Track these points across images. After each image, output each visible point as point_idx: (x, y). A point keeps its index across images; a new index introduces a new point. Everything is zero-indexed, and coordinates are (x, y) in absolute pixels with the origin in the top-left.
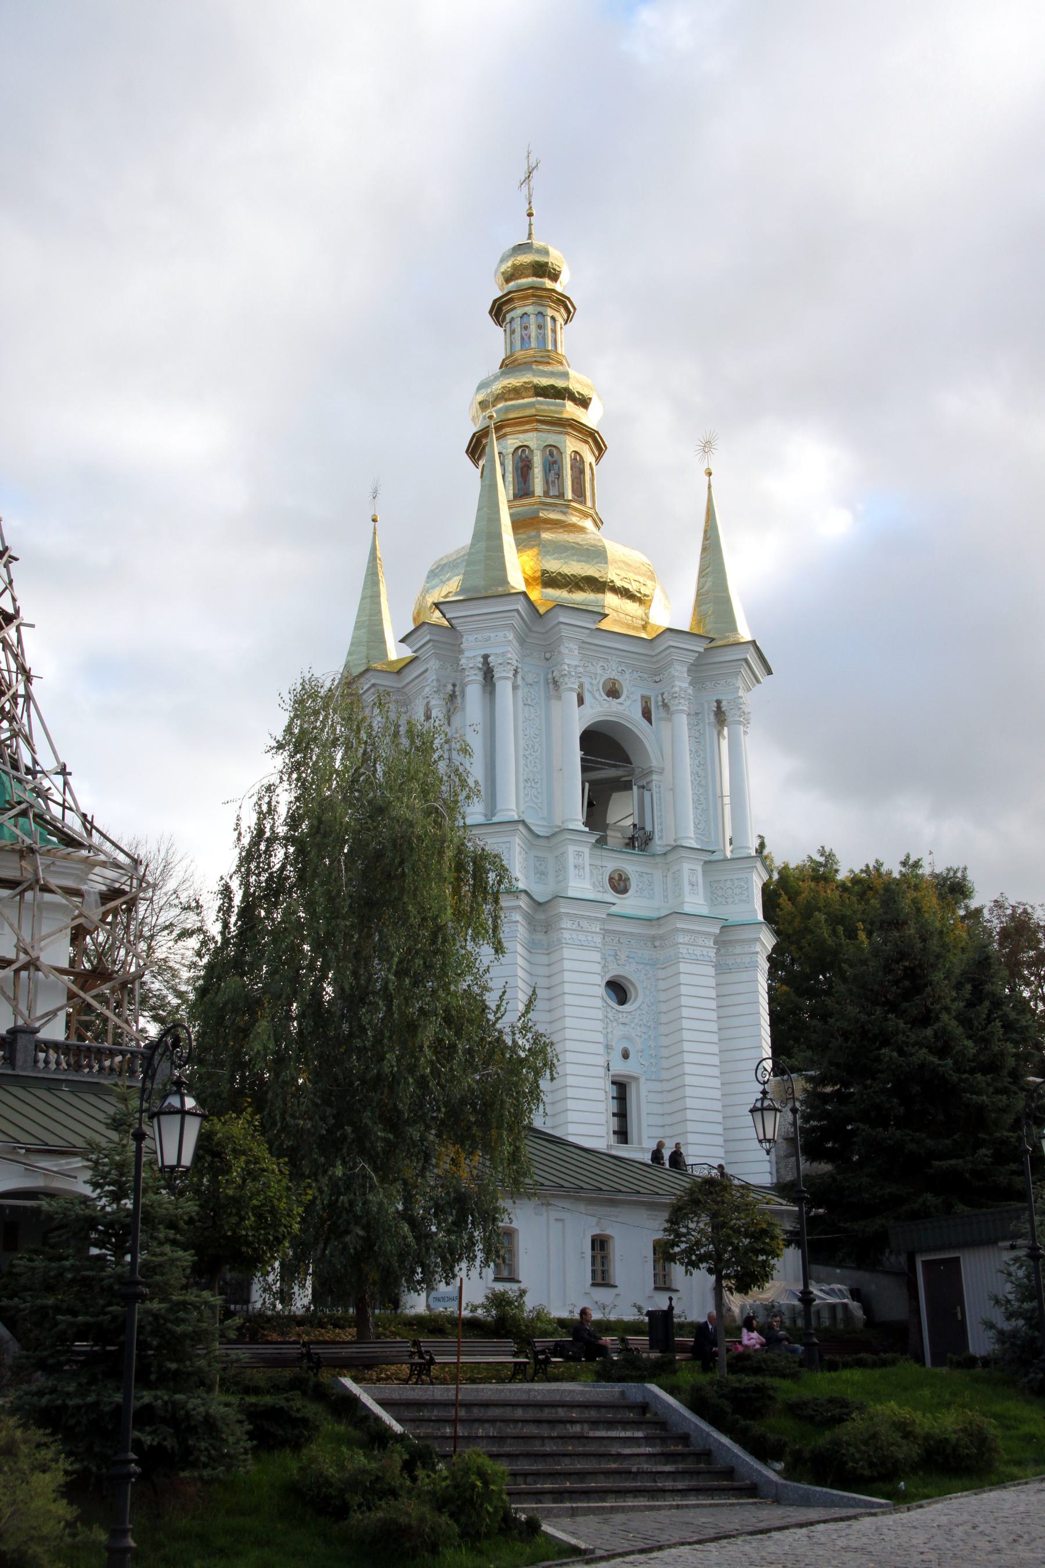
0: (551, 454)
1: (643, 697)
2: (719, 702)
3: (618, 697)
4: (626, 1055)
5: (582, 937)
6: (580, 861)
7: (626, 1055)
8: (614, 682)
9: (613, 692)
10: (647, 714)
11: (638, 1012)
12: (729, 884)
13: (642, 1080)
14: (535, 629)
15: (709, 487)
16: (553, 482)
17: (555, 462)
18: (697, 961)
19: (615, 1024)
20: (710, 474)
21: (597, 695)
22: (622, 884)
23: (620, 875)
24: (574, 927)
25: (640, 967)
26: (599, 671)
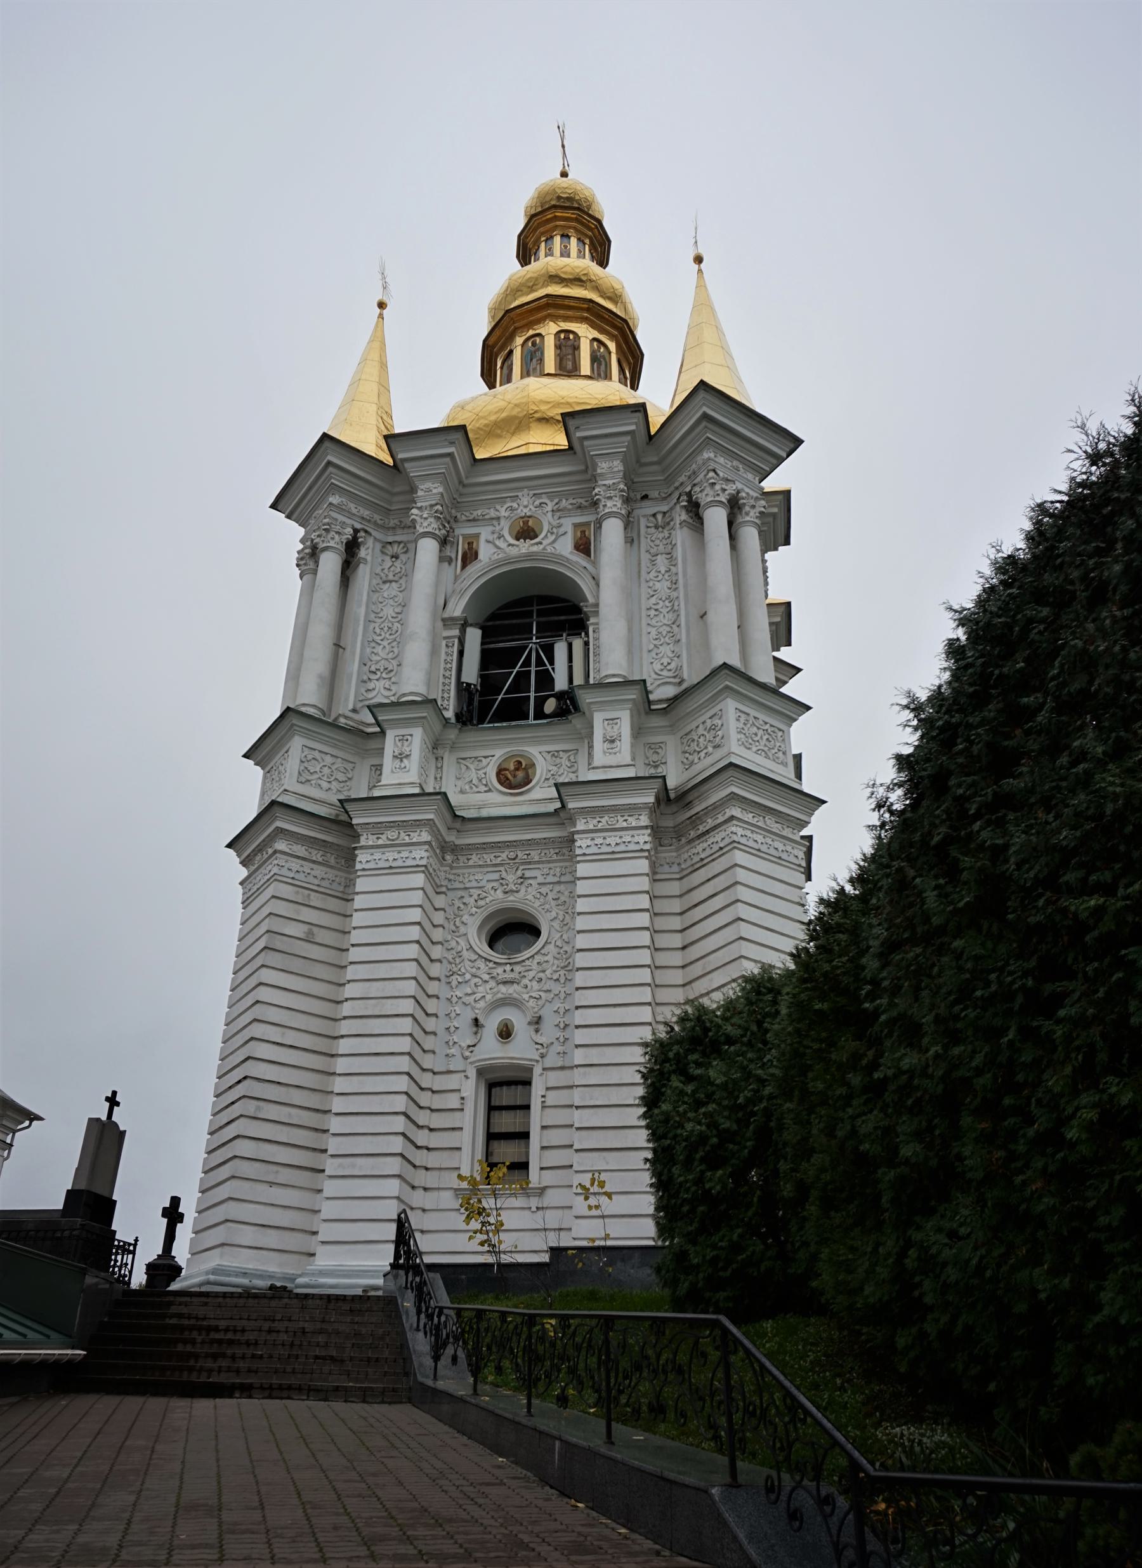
0: (534, 344)
1: (576, 526)
2: (689, 494)
3: (536, 536)
4: (505, 1033)
5: (391, 855)
6: (406, 750)
7: (505, 1033)
8: (526, 519)
9: (526, 532)
10: (584, 546)
11: (538, 958)
12: (701, 731)
13: (537, 1071)
14: (397, 490)
15: (700, 271)
16: (535, 369)
17: (538, 350)
18: (613, 856)
19: (492, 983)
20: (699, 260)
21: (501, 544)
22: (520, 774)
23: (520, 763)
24: (380, 842)
25: (544, 890)
26: (503, 513)
